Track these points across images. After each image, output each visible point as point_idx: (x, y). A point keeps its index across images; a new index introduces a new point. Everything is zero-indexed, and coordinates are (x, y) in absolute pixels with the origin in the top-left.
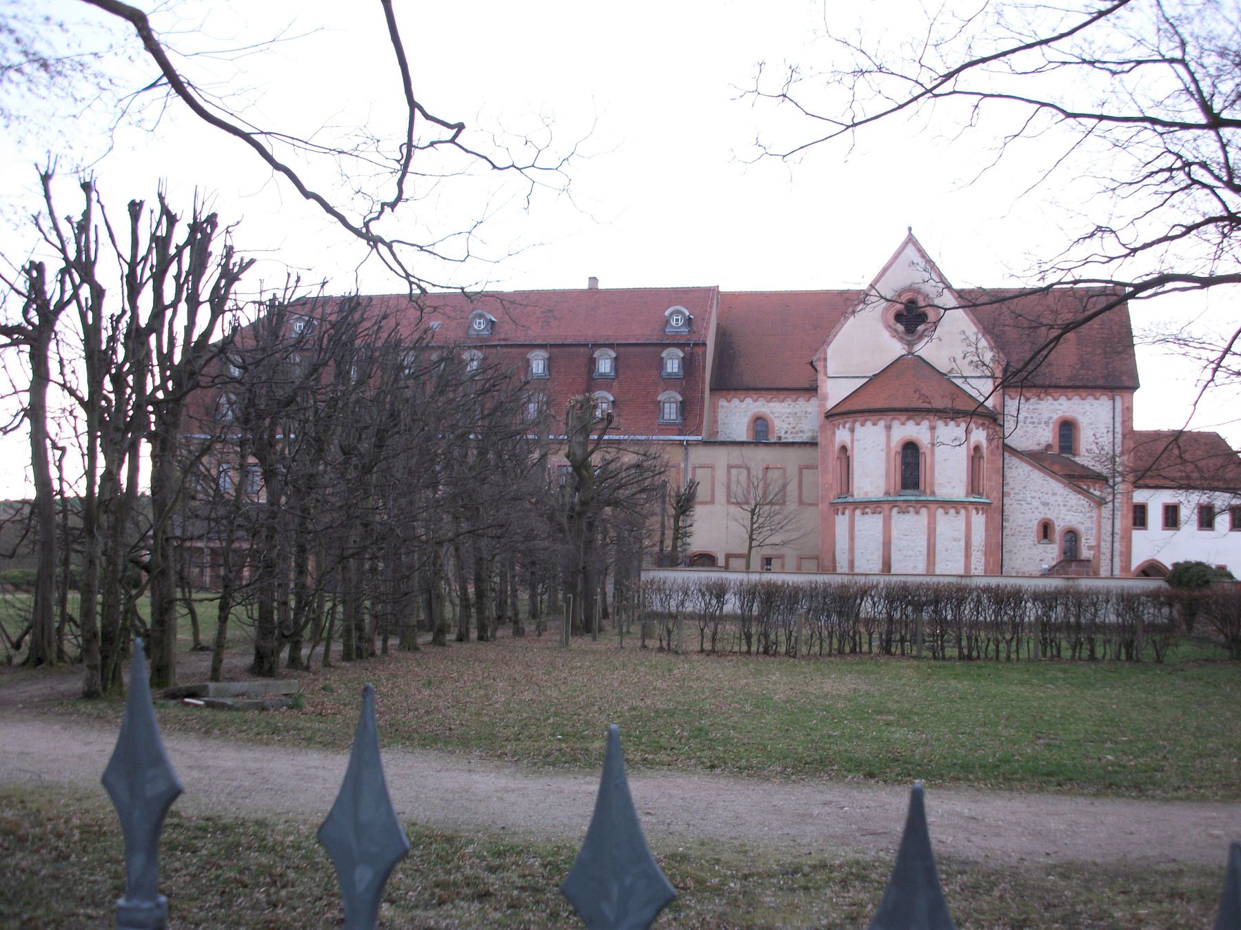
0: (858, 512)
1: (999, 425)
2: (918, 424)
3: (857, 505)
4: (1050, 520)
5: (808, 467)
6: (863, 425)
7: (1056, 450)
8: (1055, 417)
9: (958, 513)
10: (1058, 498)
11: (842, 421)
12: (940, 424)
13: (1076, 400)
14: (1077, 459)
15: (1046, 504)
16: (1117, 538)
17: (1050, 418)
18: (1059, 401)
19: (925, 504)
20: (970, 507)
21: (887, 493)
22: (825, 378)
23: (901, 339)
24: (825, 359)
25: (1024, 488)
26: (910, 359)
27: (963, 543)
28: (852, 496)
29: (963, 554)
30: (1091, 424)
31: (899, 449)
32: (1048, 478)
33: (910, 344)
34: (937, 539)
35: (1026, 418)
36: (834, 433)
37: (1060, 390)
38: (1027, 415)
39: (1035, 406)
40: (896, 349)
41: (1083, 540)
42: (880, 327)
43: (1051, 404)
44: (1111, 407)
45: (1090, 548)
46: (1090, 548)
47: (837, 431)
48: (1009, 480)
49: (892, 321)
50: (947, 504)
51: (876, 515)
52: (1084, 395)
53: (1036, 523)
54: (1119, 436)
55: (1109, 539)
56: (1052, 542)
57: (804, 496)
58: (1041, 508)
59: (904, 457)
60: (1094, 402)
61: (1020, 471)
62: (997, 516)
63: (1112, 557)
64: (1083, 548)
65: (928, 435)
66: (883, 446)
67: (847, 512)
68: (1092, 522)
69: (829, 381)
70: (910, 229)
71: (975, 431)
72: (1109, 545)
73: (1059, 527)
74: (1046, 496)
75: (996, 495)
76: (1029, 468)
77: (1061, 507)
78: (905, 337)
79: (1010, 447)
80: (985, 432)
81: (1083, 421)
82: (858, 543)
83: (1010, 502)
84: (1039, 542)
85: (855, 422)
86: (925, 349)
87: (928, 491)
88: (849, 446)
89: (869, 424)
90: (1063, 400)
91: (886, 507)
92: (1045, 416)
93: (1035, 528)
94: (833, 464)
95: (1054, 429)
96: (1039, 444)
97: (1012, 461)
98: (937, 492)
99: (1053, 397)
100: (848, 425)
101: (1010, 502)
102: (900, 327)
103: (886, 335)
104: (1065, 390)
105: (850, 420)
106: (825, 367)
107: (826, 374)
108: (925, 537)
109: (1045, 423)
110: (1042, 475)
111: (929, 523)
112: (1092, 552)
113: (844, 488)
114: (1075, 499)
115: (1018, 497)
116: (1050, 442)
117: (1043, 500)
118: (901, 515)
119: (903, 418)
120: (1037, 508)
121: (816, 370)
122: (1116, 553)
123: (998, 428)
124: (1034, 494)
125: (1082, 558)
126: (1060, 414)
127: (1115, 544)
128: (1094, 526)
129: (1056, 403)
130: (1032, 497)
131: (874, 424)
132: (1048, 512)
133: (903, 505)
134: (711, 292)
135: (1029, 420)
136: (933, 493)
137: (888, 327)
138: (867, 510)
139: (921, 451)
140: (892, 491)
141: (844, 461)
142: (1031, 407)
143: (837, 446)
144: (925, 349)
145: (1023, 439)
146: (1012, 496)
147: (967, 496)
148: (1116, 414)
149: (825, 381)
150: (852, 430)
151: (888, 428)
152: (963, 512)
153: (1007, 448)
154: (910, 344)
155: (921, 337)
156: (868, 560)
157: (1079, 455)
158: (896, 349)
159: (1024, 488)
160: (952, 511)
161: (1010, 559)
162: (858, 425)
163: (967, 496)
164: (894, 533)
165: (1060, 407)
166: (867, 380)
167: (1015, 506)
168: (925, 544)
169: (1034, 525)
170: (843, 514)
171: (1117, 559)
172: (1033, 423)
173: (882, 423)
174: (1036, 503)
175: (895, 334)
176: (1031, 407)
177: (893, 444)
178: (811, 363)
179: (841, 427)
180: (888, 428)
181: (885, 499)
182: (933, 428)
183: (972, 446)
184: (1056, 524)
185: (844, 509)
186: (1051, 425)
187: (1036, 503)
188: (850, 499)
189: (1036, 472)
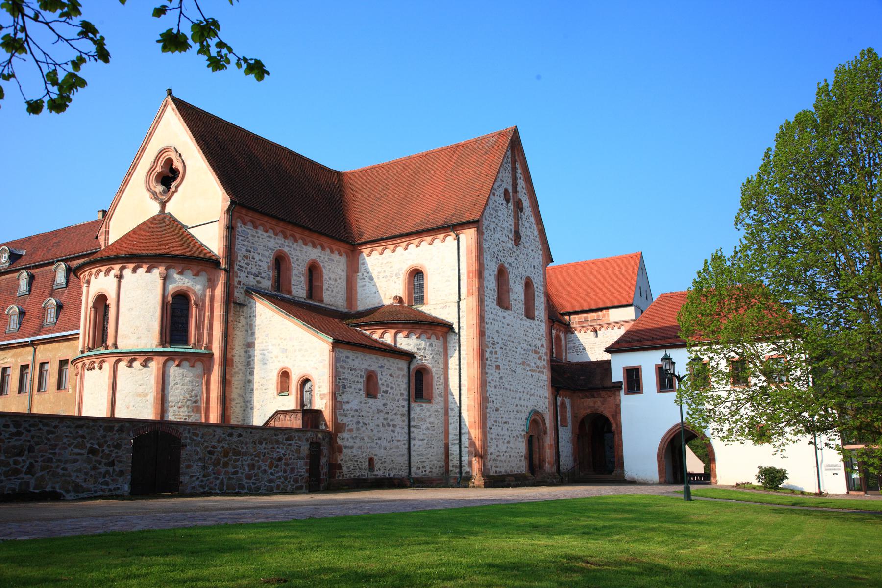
4: (287, 368)
9: (145, 365)
15: (285, 351)
23: (156, 199)
35: (379, 273)
40: (154, 209)
43: (402, 255)
45: (322, 396)
50: (132, 356)
102: (159, 188)
116: (401, 295)
120: (277, 357)
148: (461, 254)
154: (163, 205)
157: (427, 304)
159: (267, 335)
172: (386, 277)
175: (155, 196)
184: (292, 370)
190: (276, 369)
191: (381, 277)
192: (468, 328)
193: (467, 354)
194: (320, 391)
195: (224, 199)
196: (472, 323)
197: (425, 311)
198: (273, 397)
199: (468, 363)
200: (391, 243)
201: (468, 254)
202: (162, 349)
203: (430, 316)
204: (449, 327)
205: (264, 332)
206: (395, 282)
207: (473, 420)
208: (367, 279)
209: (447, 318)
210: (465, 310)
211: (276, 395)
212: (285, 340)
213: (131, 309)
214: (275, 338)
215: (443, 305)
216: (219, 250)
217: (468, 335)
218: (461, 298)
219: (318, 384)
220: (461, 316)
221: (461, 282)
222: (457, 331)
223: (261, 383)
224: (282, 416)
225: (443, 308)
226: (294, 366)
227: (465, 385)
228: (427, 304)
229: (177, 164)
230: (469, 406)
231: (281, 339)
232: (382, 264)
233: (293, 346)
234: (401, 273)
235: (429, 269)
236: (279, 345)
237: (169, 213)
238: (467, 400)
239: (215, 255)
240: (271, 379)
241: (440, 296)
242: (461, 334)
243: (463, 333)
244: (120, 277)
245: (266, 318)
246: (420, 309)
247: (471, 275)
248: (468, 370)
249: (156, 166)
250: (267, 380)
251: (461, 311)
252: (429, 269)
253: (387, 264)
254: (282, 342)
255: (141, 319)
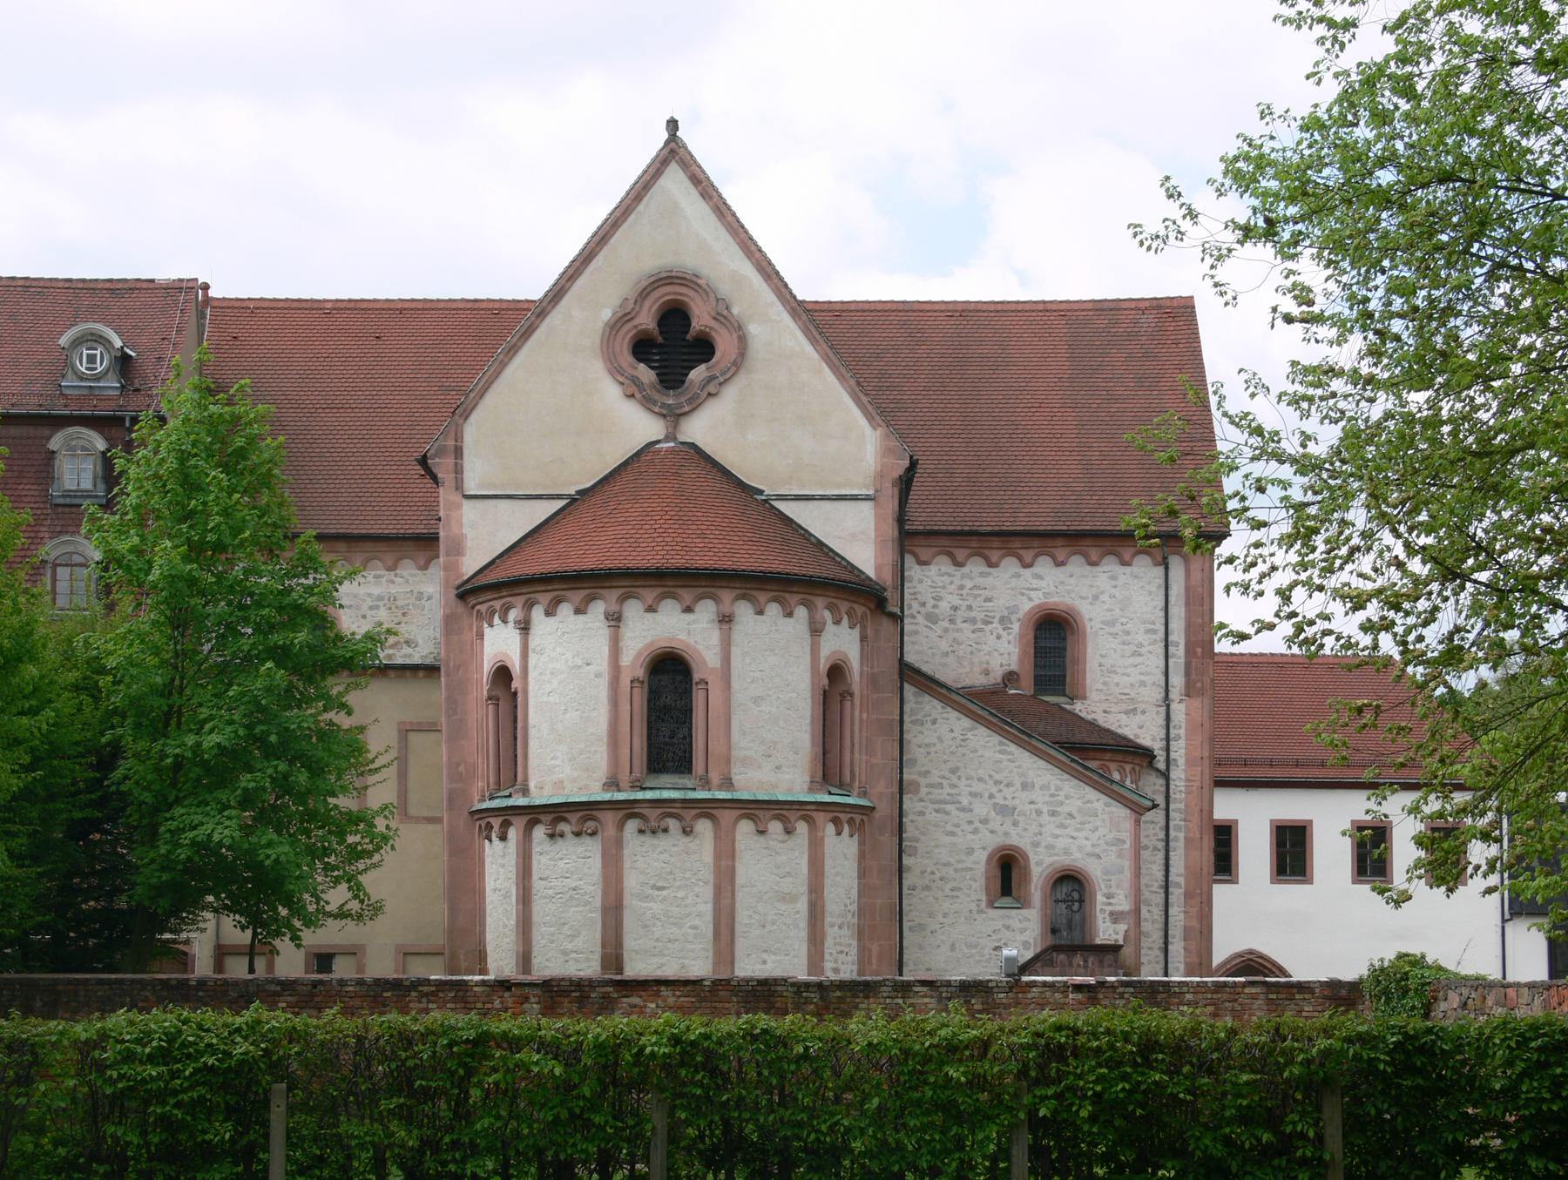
0: (539, 832)
1: (892, 616)
2: (688, 610)
3: (534, 814)
5: (421, 728)
6: (549, 613)
7: (1026, 687)
8: (1026, 606)
10: (1037, 795)
11: (497, 604)
12: (744, 611)
13: (1076, 566)
14: (1078, 707)
15: (1004, 810)
16: (1177, 895)
17: (1013, 609)
18: (1037, 569)
19: (707, 809)
20: (820, 817)
21: (612, 783)
22: (456, 497)
23: (647, 403)
24: (458, 452)
25: (954, 771)
26: (670, 451)
27: (802, 905)
28: (525, 791)
29: (804, 934)
30: (1112, 623)
31: (640, 673)
32: (1012, 748)
33: (674, 417)
34: (739, 895)
35: (955, 609)
36: (481, 636)
37: (1036, 543)
38: (956, 601)
39: (980, 581)
40: (642, 427)
41: (1100, 898)
42: (597, 370)
43: (1018, 576)
44: (1162, 581)
45: (1116, 917)
46: (1116, 917)
47: (487, 630)
48: (914, 751)
49: (627, 358)
51: (587, 840)
52: (1094, 553)
53: (982, 856)
54: (1179, 652)
55: (1160, 898)
56: (1023, 903)
57: (413, 798)
58: (996, 821)
59: (654, 695)
60: (1119, 569)
61: (942, 729)
62: (888, 841)
63: (1166, 943)
64: (1100, 916)
65: (715, 637)
66: (602, 663)
67: (512, 833)
68: (1120, 855)
69: (468, 506)
70: (673, 125)
71: (830, 628)
72: (1158, 913)
73: (1040, 866)
74: (1008, 792)
75: (882, 789)
76: (966, 722)
77: (1045, 818)
78: (657, 396)
79: (918, 672)
80: (856, 633)
81: (1092, 616)
82: (541, 910)
83: (919, 806)
84: (991, 904)
85: (529, 606)
86: (702, 429)
87: (715, 777)
88: (516, 669)
89: (565, 610)
90: (1044, 566)
91: (609, 818)
92: (1002, 602)
93: (981, 868)
94: (479, 714)
95: (1022, 636)
96: (986, 672)
97: (921, 706)
98: (736, 778)
99: (1020, 558)
100: (513, 615)
101: (919, 806)
102: (646, 374)
103: (611, 391)
104: (1049, 542)
105: (519, 601)
106: (458, 470)
107: (459, 486)
108: (708, 892)
109: (1002, 620)
110: (996, 738)
111: (718, 856)
112: (1122, 927)
113: (506, 775)
114: (1076, 796)
115: (938, 794)
116: (1014, 667)
117: (999, 800)
118: (648, 840)
119: (650, 595)
120: (985, 821)
121: (434, 478)
122: (1176, 932)
123: (886, 625)
124: (977, 787)
125: (1098, 941)
126: (1038, 599)
127: (1172, 912)
128: (1127, 864)
129: (1027, 572)
130: (974, 795)
131: (579, 611)
132: (1013, 831)
133: (652, 814)
134: (187, 294)
135: (961, 614)
136: (728, 783)
137: (615, 370)
138: (563, 827)
139: (696, 677)
140: (625, 778)
141: (504, 705)
142: (969, 584)
143: (487, 666)
144: (702, 429)
145: (951, 660)
146: (923, 791)
147: (811, 790)
148: (1172, 599)
149: (459, 506)
150: (525, 627)
151: (615, 619)
152: (802, 828)
153: (908, 674)
154: (674, 417)
155: (695, 404)
156: (565, 953)
157: (1084, 698)
158: (642, 427)
159: (954, 771)
160: (775, 827)
161: (921, 947)
162: (537, 613)
163: (811, 790)
164: (631, 882)
165: (1036, 583)
166: (560, 504)
167: (933, 817)
168: (707, 909)
169: (979, 863)
170: (503, 838)
171: (1177, 947)
172: (973, 621)
173: (598, 609)
174: (981, 809)
175: (634, 391)
176: (969, 584)
177: (626, 660)
178: (423, 461)
179: (496, 620)
180: (615, 619)
181: (607, 797)
182: (726, 620)
183: (824, 666)
184: (1033, 859)
185: (506, 825)
186: (1016, 627)
187: (981, 809)
188: (521, 801)
189: (982, 731)
190: (984, 848)
191: (959, 621)
192: (1190, 762)
193: (1185, 820)
194: (1110, 904)
195: (887, 451)
196: (1198, 754)
197: (1083, 715)
198: (974, 908)
199: (1186, 838)
200: (996, 544)
201: (1187, 604)
202: (827, 798)
203: (1093, 725)
204: (1140, 756)
205: (945, 762)
206: (999, 637)
207: (1196, 960)
208: (920, 619)
209: (1137, 736)
210: (1183, 725)
211: (983, 905)
212: (1008, 785)
213: (757, 700)
214: (980, 780)
215: (1124, 707)
216: (878, 568)
217: (1188, 780)
218: (1171, 696)
219: (1105, 891)
220: (1172, 736)
221: (1171, 661)
222: (1161, 766)
223: (938, 875)
224: (1062, 957)
225: (1127, 713)
226: (1036, 845)
227: (1178, 885)
228: (1084, 698)
229: (701, 319)
230: (1186, 929)
231: (997, 783)
232: (961, 587)
233: (1032, 803)
234: (1013, 618)
235: (1091, 620)
236: (991, 796)
237: (693, 446)
238: (1182, 916)
239: (868, 578)
240: (971, 869)
241: (1117, 684)
242: (1173, 775)
243: (1177, 774)
244: (726, 620)
245: (952, 731)
246: (1068, 707)
247: (1199, 650)
248: (1186, 855)
249: (638, 313)
250: (956, 870)
251: (1171, 725)
252: (1091, 620)
253: (976, 592)
254: (1000, 791)
255: (781, 723)
